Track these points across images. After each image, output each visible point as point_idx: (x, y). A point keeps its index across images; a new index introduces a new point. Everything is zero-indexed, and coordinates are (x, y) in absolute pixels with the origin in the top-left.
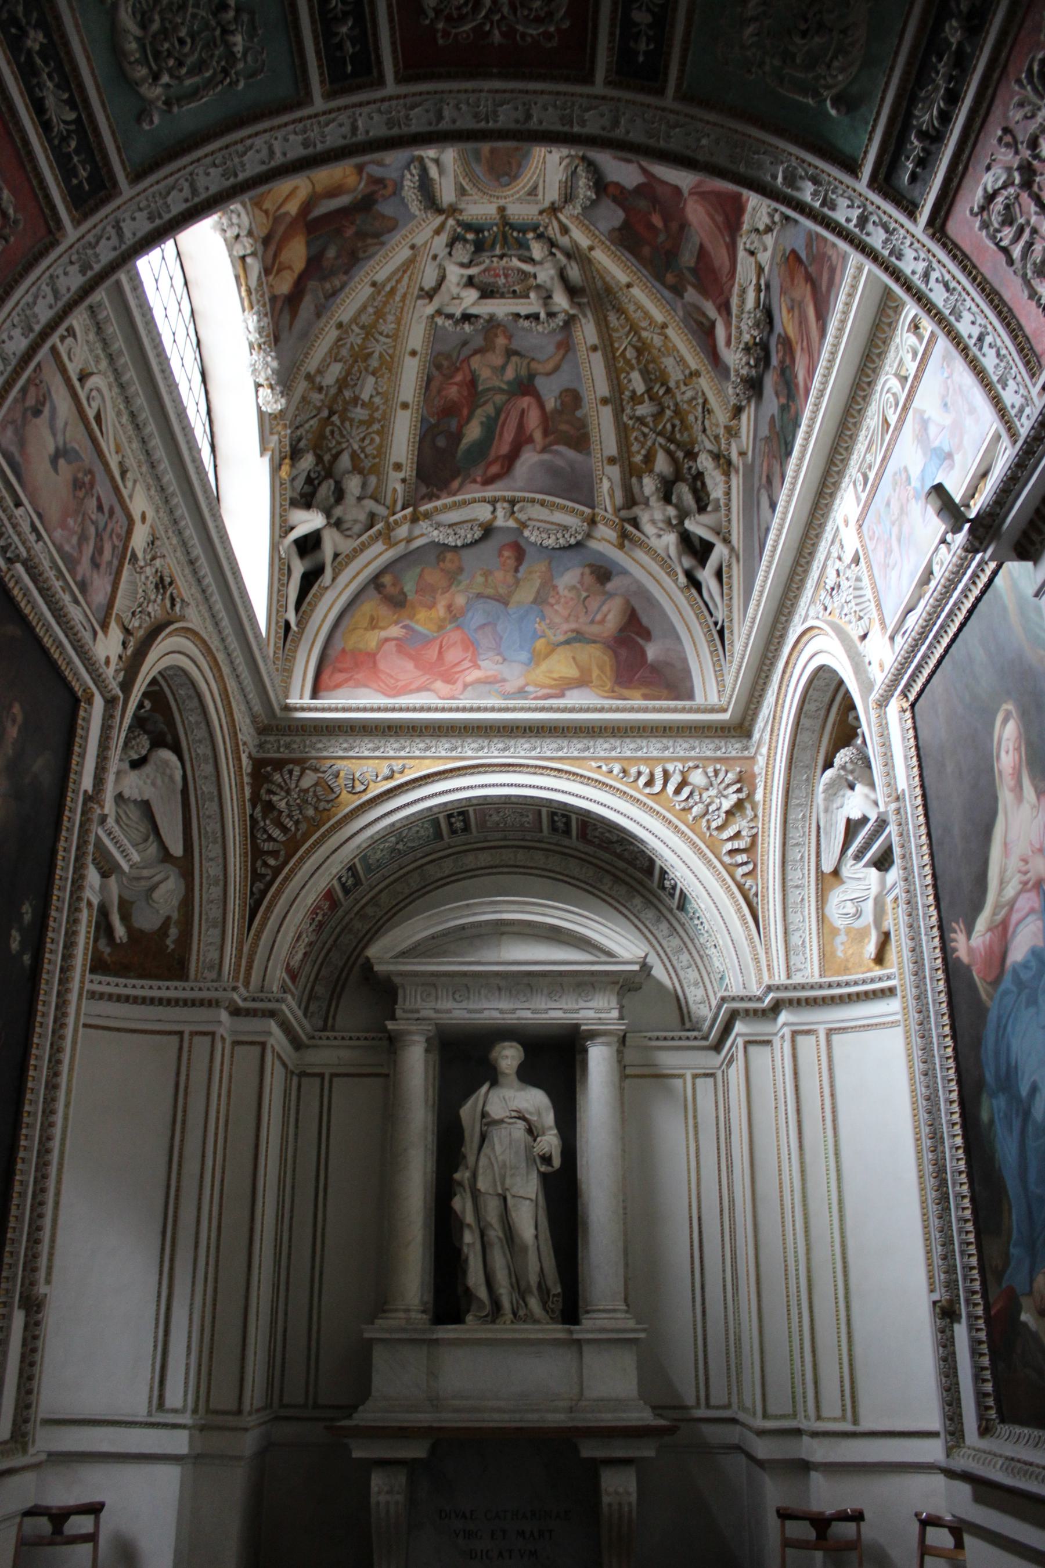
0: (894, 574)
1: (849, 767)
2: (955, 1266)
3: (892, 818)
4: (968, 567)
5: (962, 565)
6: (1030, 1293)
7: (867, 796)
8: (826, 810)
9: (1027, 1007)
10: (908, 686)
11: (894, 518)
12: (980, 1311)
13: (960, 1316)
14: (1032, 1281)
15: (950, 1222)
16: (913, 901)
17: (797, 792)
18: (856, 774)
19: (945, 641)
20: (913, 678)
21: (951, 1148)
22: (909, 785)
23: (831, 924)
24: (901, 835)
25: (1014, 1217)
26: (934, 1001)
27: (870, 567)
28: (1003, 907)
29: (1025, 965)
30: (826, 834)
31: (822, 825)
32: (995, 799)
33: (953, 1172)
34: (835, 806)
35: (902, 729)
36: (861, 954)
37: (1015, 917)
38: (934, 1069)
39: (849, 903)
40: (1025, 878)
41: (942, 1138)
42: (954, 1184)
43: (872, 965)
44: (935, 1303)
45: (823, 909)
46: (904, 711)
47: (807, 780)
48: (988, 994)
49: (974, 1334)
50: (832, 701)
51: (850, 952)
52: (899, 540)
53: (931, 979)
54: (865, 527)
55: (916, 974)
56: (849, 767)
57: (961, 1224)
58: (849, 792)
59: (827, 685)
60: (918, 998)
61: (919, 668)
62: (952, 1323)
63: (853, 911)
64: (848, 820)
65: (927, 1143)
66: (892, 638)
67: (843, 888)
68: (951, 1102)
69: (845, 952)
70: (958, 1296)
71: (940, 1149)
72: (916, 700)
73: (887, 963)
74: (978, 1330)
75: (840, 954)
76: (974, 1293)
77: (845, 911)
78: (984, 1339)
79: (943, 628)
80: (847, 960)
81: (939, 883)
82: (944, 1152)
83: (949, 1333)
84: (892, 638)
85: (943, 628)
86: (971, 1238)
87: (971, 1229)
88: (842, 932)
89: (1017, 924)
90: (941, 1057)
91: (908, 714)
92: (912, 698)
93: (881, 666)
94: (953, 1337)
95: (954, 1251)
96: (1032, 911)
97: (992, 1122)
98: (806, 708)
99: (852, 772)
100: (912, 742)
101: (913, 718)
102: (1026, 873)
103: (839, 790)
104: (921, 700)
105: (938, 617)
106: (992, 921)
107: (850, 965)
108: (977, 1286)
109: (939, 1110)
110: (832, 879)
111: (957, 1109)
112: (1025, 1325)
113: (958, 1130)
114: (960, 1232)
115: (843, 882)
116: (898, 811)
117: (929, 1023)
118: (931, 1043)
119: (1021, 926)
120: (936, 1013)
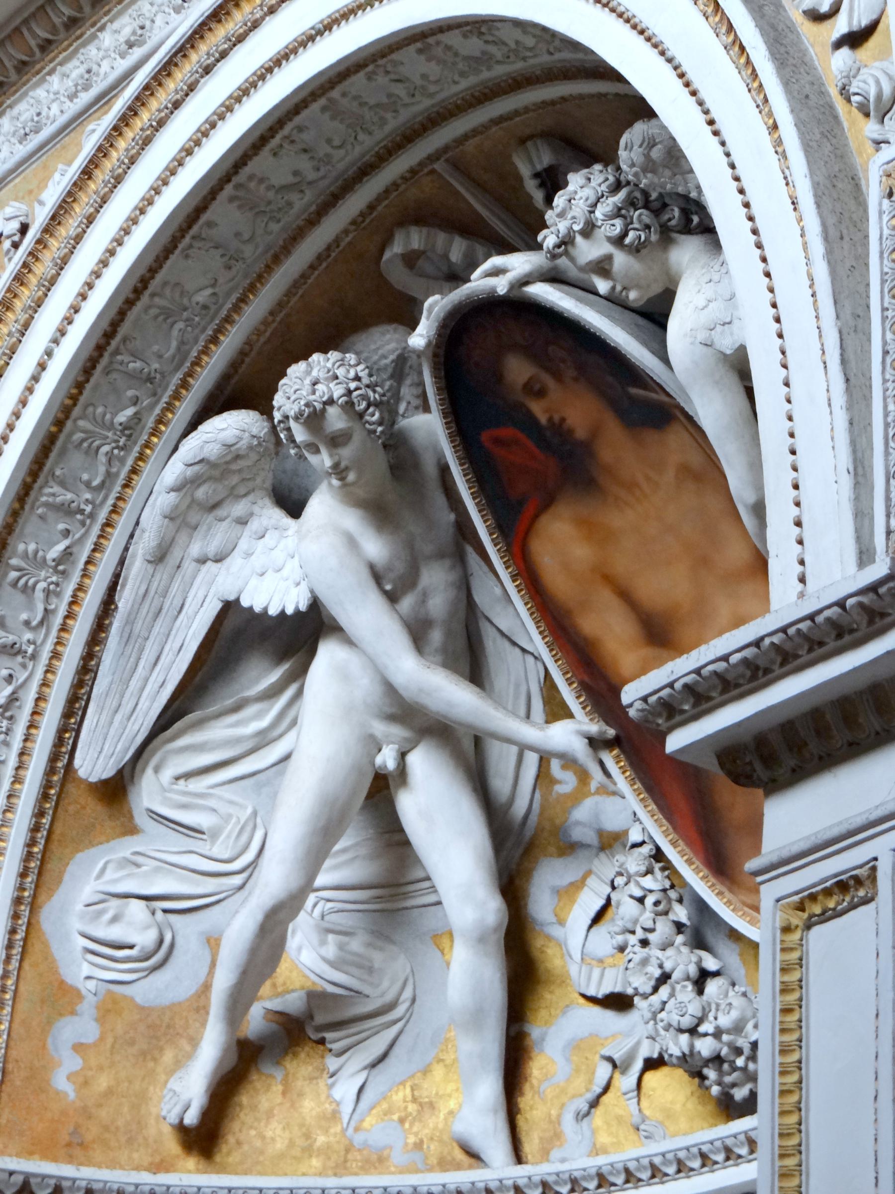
1: (336, 420)
7: (352, 543)
8: (159, 557)
17: (76, 459)
18: (346, 453)
23: (53, 969)
30: (127, 639)
31: (124, 600)
34: (195, 549)
36: (141, 1099)
39: (137, 908)
43: (172, 1146)
45: (34, 907)
47: (129, 429)
50: (365, 171)
51: (103, 1082)
56: (336, 420)
58: (275, 515)
59: (393, 104)
63: (145, 939)
64: (229, 608)
67: (126, 847)
69: (82, 1081)
73: (228, 1151)
75: (61, 1082)
77: (115, 933)
80: (86, 1113)
88: (87, 1007)
98: (261, 164)
99: (336, 441)
103: (234, 495)
107: (92, 1132)
110: (94, 808)
115: (131, 830)
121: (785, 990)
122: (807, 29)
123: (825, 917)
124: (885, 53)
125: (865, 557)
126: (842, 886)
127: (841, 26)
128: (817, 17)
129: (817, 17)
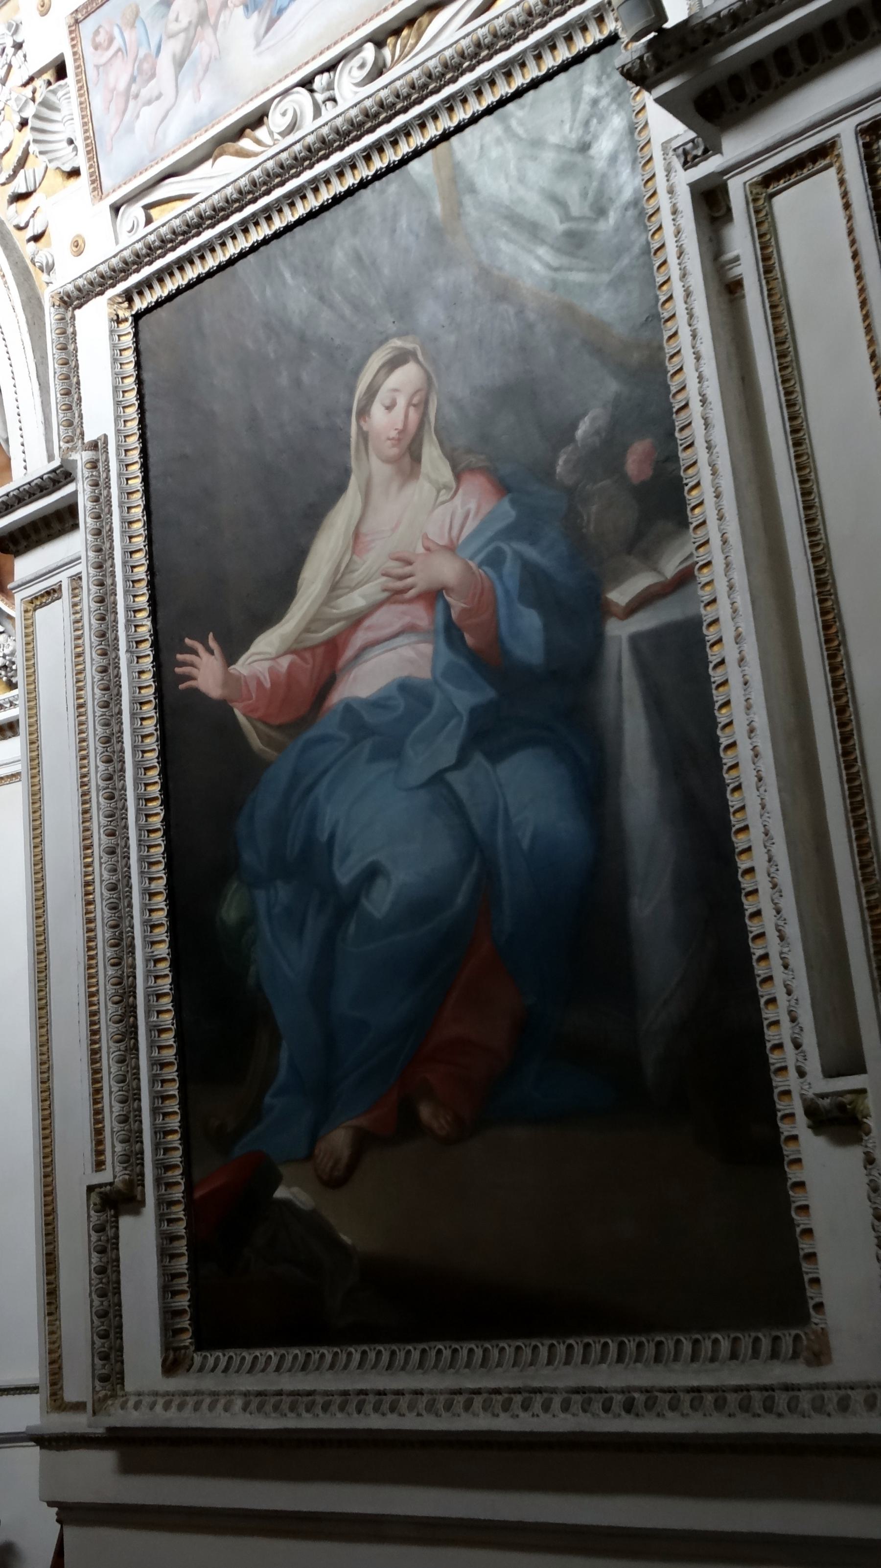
0: (148, 115)
2: (140, 1131)
3: (81, 472)
4: (372, 130)
5: (361, 124)
6: (310, 1156)
9: (374, 758)
10: (147, 284)
11: (174, 27)
12: (178, 1193)
13: (142, 1203)
14: (314, 1138)
15: (137, 1067)
16: (109, 599)
19: (264, 231)
20: (160, 276)
21: (147, 961)
22: (118, 432)
24: (96, 500)
25: (284, 1056)
26: (135, 748)
27: (83, 89)
28: (332, 622)
29: (378, 703)
32: (347, 473)
33: (147, 996)
35: (114, 347)
37: (360, 638)
38: (127, 846)
40: (399, 584)
41: (132, 946)
42: (148, 1014)
44: (90, 1189)
46: (119, 321)
48: (268, 741)
49: (165, 1226)
52: (179, 64)
53: (133, 715)
54: (87, 28)
55: (106, 705)
57: (156, 1070)
60: (107, 740)
61: (180, 265)
62: (116, 1216)
65: (104, 952)
66: (116, 209)
68: (152, 895)
70: (142, 1174)
71: (128, 961)
72: (149, 310)
74: (171, 1221)
76: (169, 1168)
78: (183, 1232)
79: (267, 214)
81: (157, 580)
82: (133, 966)
83: (110, 1232)
84: (116, 209)
85: (267, 214)
86: (173, 1089)
87: (174, 1076)
89: (364, 649)
90: (140, 829)
91: (127, 327)
92: (140, 304)
93: (78, 247)
94: (117, 1237)
95: (139, 1109)
96: (410, 629)
97: (248, 921)
100: (130, 368)
101: (136, 335)
102: (401, 578)
104: (161, 312)
105: (268, 192)
106: (297, 641)
108: (176, 1157)
109: (130, 905)
111: (163, 905)
112: (286, 1204)
113: (161, 933)
114: (153, 1080)
116: (94, 465)
117: (122, 778)
118: (125, 808)
119: (377, 650)
120: (137, 765)
121: (27, 635)
122: (15, 233)
123: (42, 606)
124: (49, 244)
125: (51, 458)
126: (48, 593)
127: (30, 233)
128: (19, 228)
129: (19, 228)
